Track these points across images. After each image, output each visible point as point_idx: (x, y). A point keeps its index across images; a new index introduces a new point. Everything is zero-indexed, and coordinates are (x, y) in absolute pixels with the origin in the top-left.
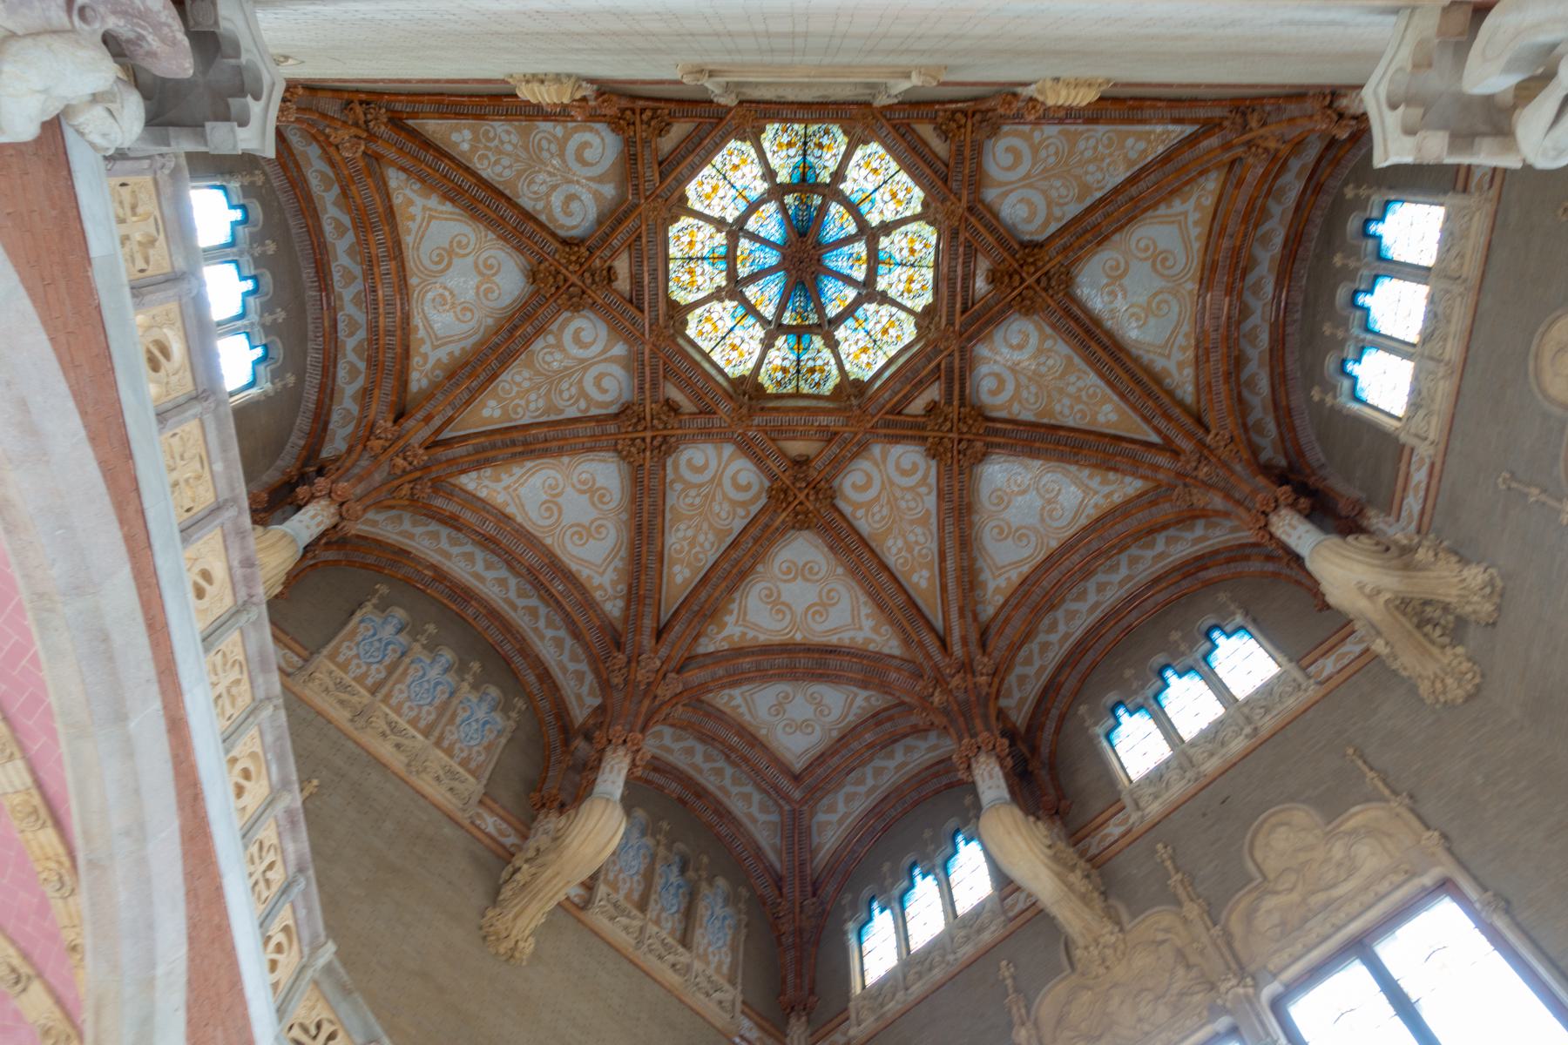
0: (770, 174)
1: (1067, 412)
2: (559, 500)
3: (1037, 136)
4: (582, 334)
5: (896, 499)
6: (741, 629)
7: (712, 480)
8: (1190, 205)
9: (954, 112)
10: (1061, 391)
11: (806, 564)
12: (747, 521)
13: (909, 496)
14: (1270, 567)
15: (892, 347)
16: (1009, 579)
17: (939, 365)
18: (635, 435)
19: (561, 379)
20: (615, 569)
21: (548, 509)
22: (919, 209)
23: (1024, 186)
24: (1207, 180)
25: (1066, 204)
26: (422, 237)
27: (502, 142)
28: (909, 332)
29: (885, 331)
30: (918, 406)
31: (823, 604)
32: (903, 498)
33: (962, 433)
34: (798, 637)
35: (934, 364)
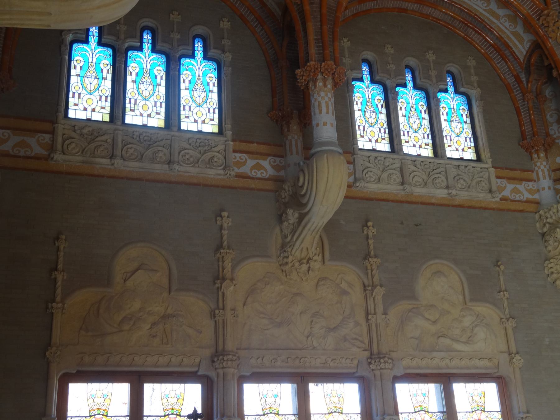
14: (511, 80)
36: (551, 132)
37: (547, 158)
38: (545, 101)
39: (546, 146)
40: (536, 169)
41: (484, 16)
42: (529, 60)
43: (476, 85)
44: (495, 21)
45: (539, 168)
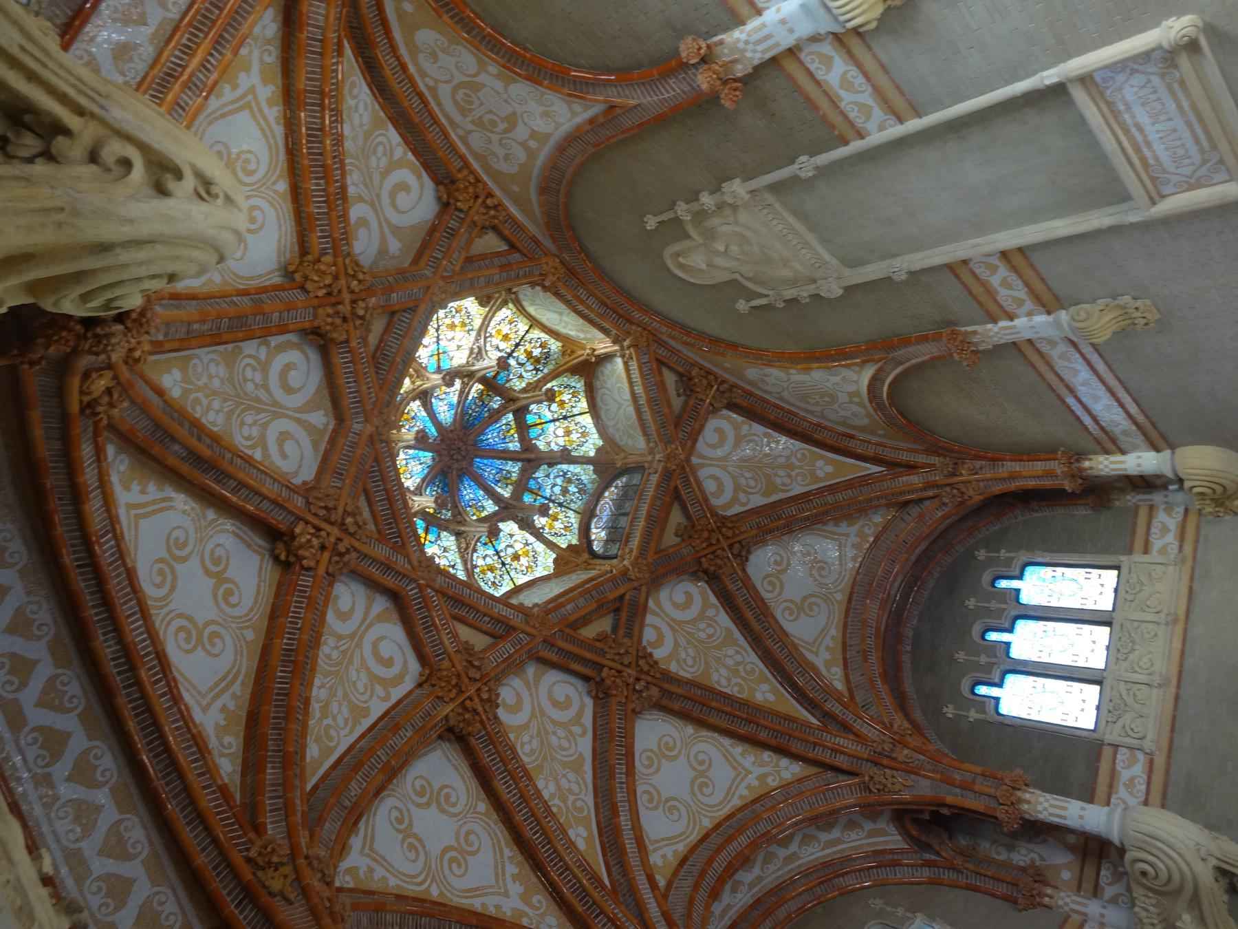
0: (478, 354)
1: (724, 682)
2: (179, 568)
3: (745, 429)
4: (293, 373)
5: (547, 732)
6: (368, 861)
7: (352, 636)
8: (853, 530)
9: (709, 373)
10: (718, 660)
11: (441, 789)
12: (387, 705)
13: (561, 733)
14: (926, 873)
15: (520, 576)
16: (664, 856)
17: (622, 597)
18: (323, 525)
19: (249, 408)
20: (224, 709)
21: (161, 572)
22: (592, 454)
23: (717, 466)
24: (875, 513)
25: (751, 493)
26: (223, 116)
27: (357, 107)
28: (546, 562)
29: (516, 557)
30: (589, 632)
31: (462, 852)
32: (554, 733)
33: (641, 671)
34: (435, 893)
35: (621, 591)
36: (1022, 864)
37: (1056, 887)
38: (974, 849)
39: (1037, 878)
40: (1066, 908)
41: (828, 855)
42: (912, 838)
43: (909, 915)
44: (839, 848)
45: (1066, 904)
